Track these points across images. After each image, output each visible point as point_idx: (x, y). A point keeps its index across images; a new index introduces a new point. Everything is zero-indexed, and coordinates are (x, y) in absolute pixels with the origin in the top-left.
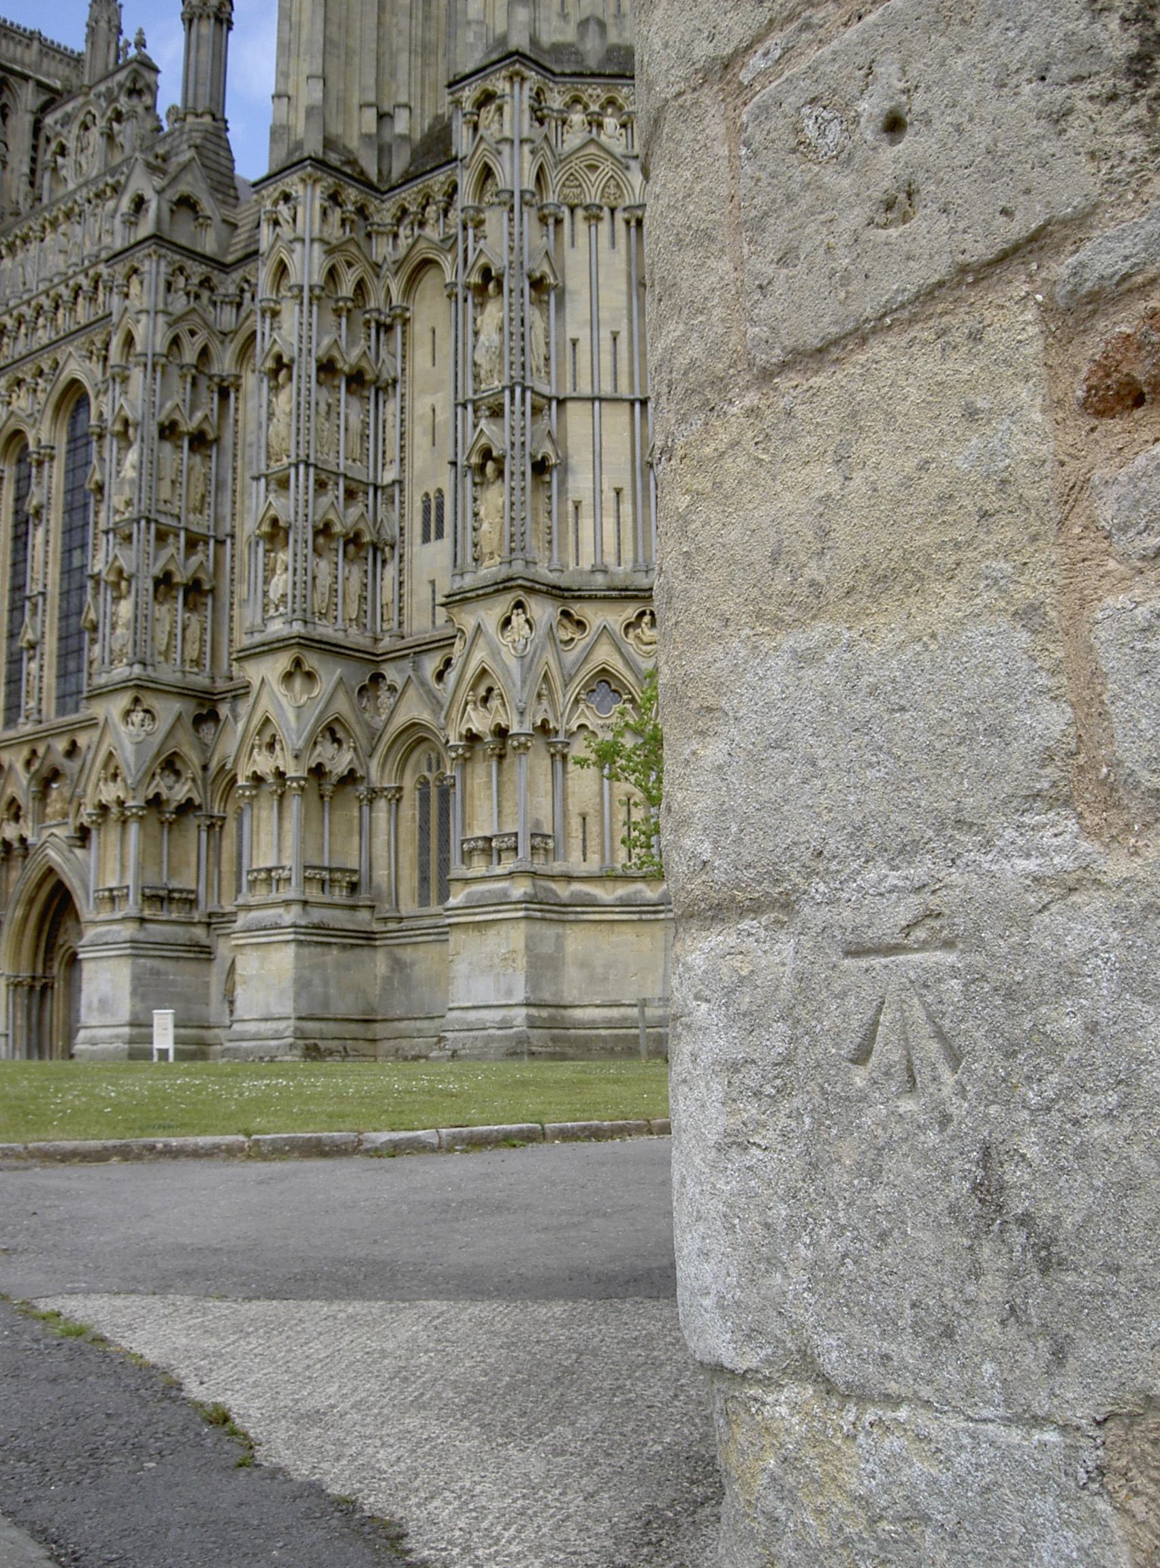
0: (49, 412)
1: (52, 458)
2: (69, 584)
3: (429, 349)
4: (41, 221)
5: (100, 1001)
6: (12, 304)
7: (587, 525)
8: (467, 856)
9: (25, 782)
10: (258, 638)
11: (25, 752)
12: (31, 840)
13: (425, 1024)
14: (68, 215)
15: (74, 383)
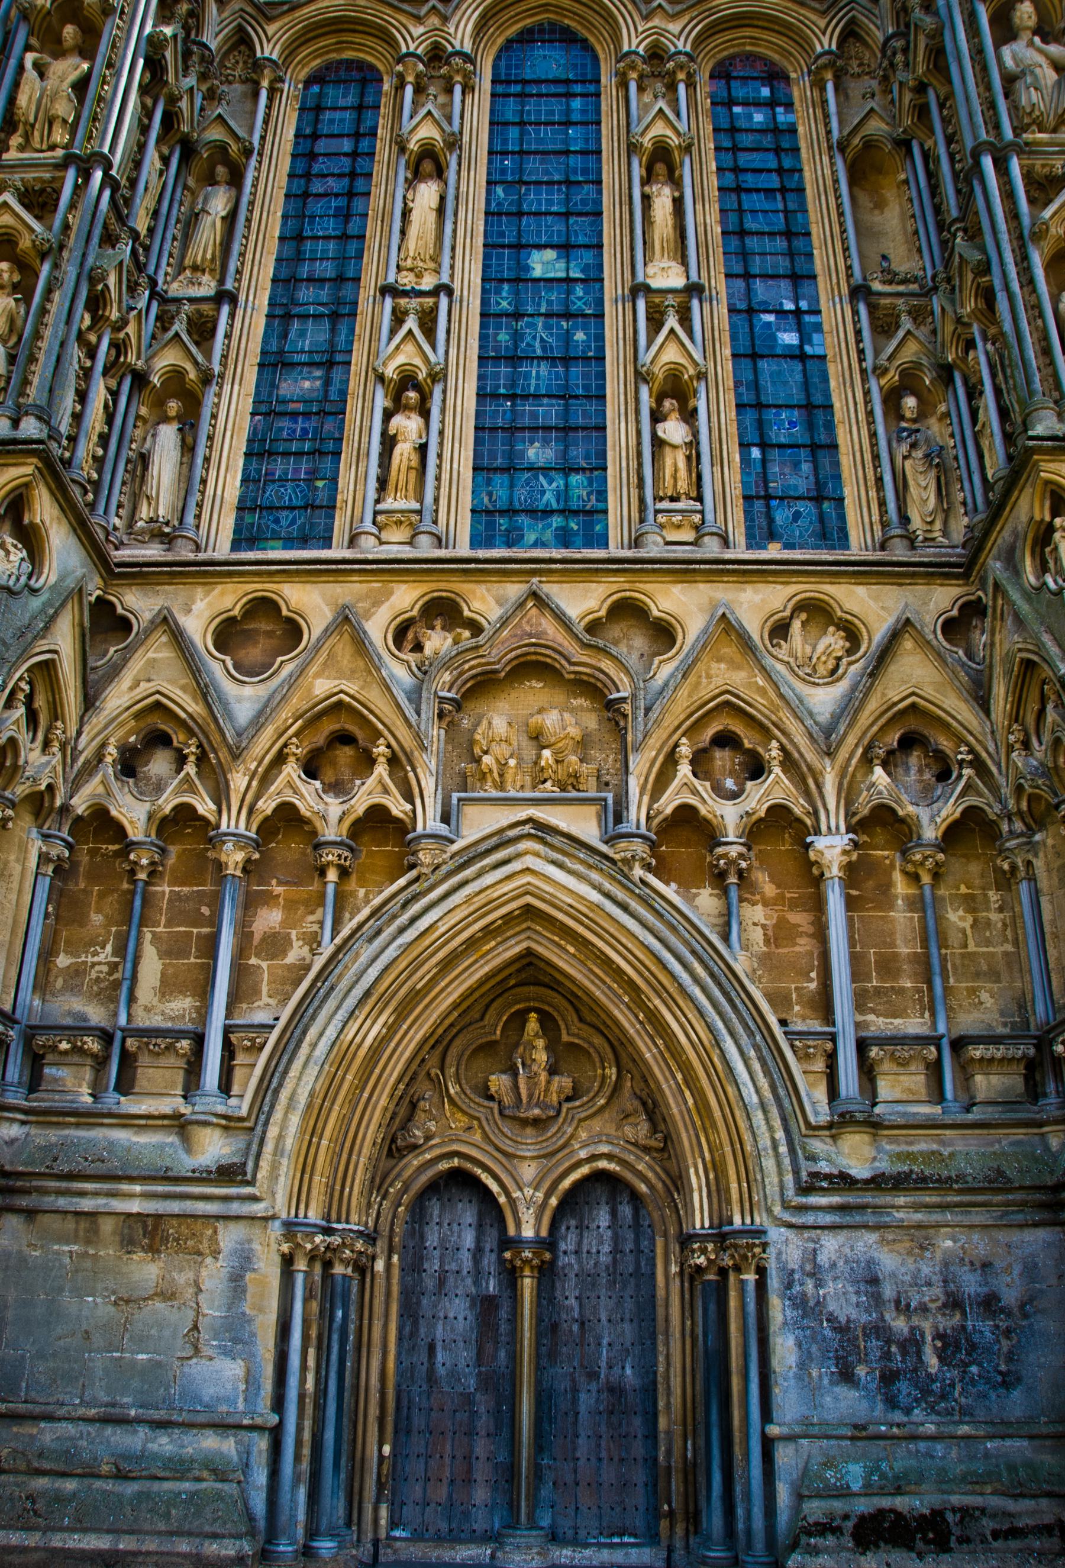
2: (518, 301)
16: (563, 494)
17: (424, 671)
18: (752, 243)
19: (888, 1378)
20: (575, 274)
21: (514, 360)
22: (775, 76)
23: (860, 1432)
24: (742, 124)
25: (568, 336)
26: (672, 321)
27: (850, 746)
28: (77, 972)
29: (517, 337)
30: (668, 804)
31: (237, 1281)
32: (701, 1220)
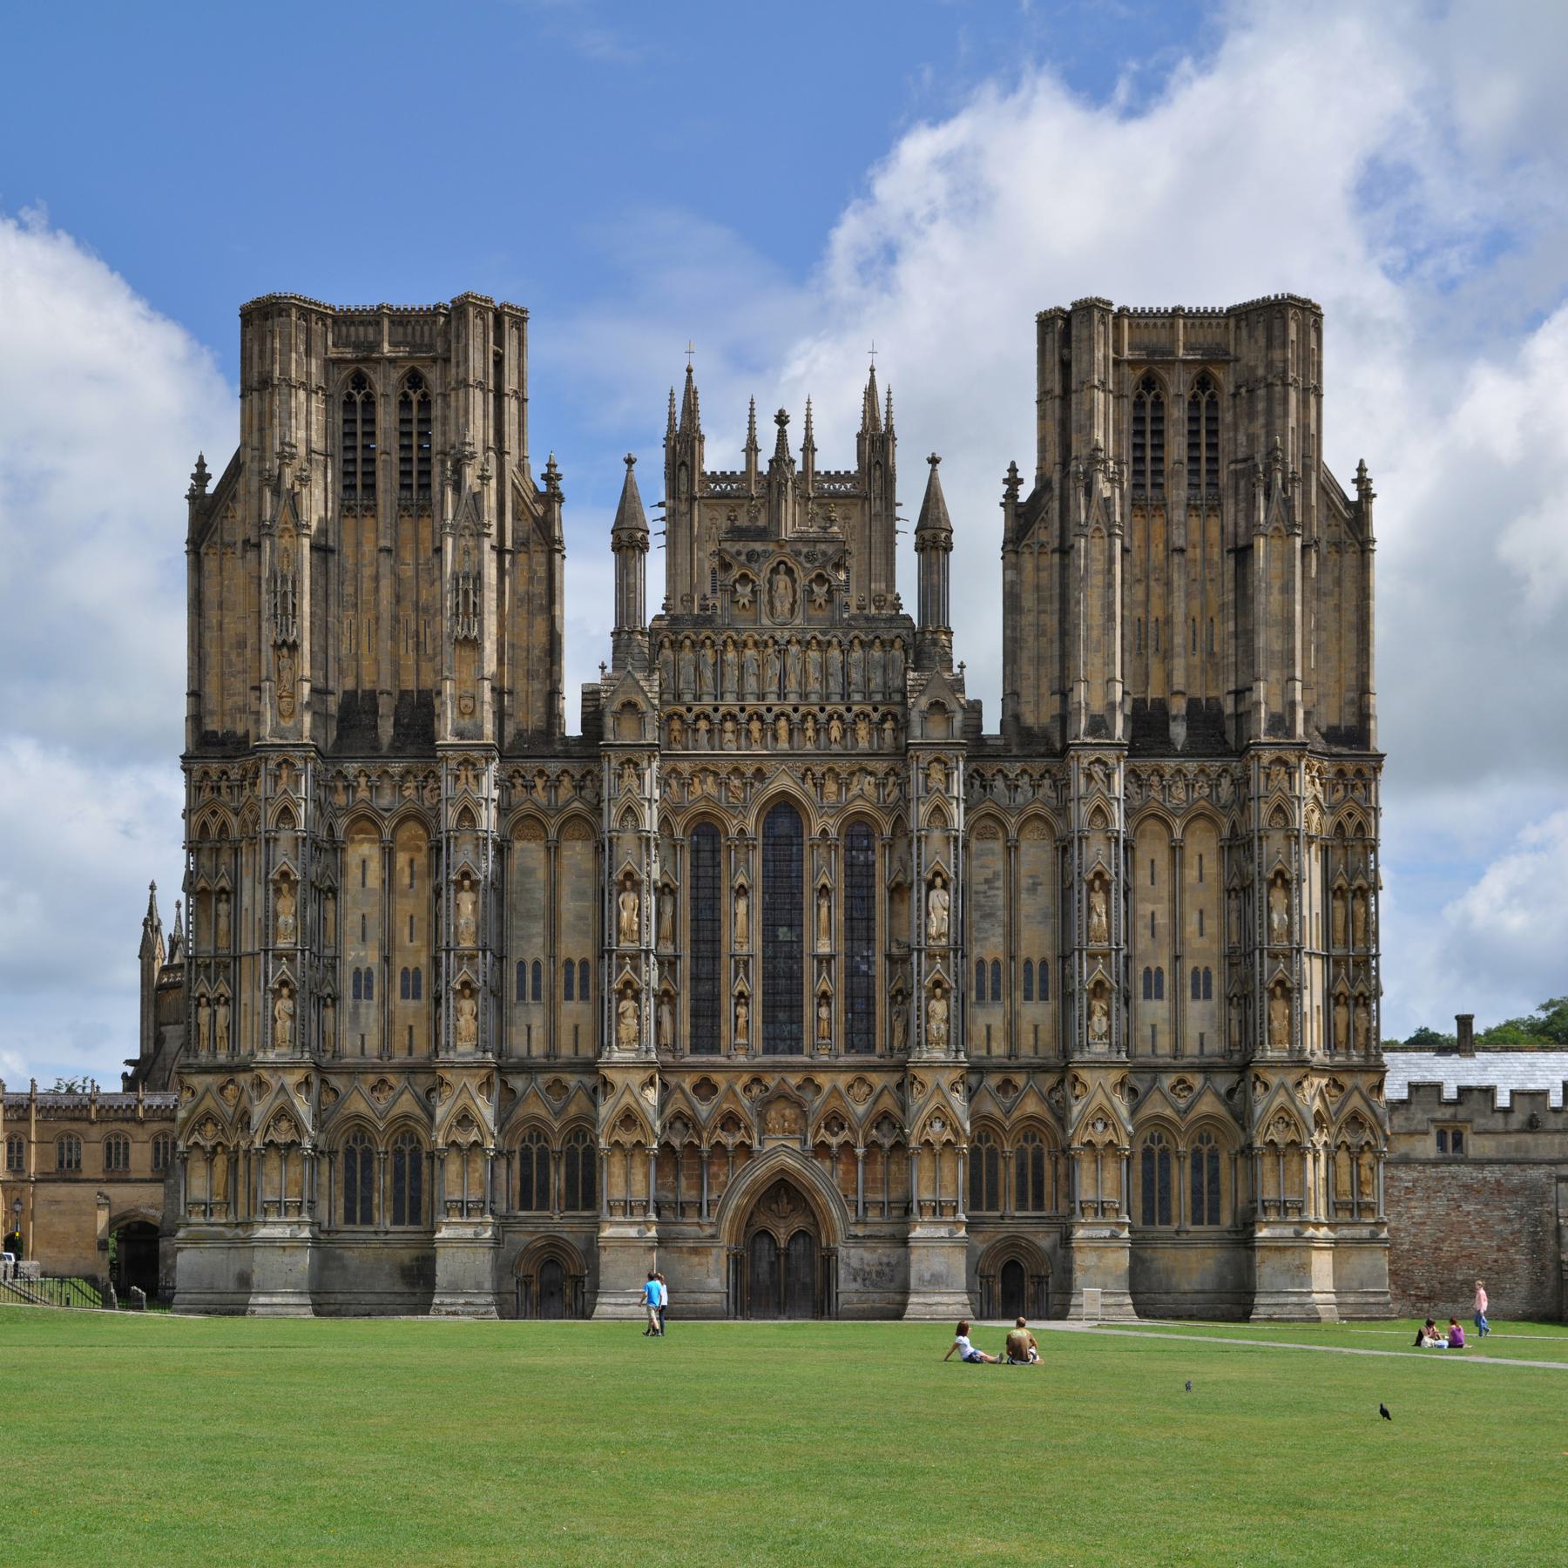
0: (755, 811)
1: (754, 847)
2: (774, 951)
3: (1149, 872)
4: (724, 637)
5: (932, 1275)
6: (688, 698)
7: (1309, 1025)
8: (1265, 1209)
9: (746, 1102)
10: (1087, 1057)
11: (746, 1078)
12: (756, 1146)
13: (1164, 1297)
14: (756, 643)
15: (783, 792)
16: (790, 1032)
17: (752, 1099)
18: (855, 923)
19: (864, 1280)
20: (794, 939)
21: (774, 978)
22: (869, 836)
23: (857, 1292)
24: (855, 861)
25: (791, 968)
26: (824, 974)
27: (867, 1125)
28: (664, 1184)
29: (775, 968)
30: (818, 1140)
31: (717, 1261)
32: (824, 1245)
